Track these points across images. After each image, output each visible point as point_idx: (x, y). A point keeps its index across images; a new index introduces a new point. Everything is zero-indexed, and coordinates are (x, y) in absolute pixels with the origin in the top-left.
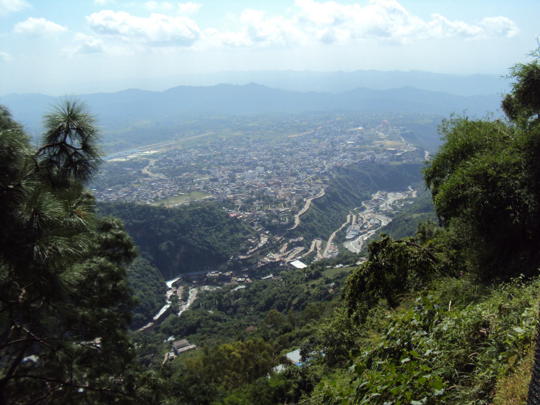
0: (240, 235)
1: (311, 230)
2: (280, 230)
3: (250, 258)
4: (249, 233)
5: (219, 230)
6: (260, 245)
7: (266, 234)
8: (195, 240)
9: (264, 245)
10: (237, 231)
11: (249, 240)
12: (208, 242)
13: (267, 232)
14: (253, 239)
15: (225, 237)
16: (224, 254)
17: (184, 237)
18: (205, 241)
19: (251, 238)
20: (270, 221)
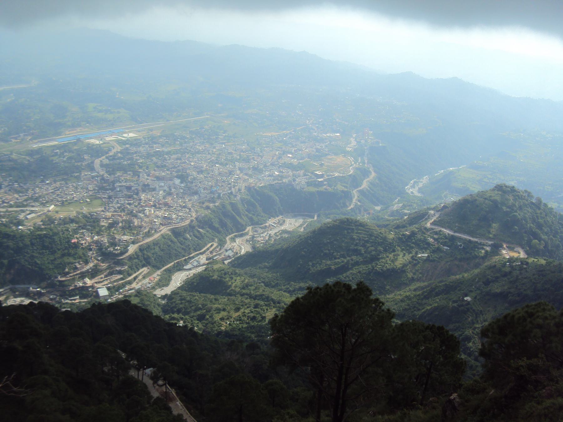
0: (71, 260)
1: (147, 258)
2: (111, 257)
3: (68, 280)
4: (80, 258)
5: (53, 253)
6: (85, 269)
7: (98, 260)
8: (26, 260)
9: (88, 270)
10: (69, 255)
11: (77, 264)
12: (37, 264)
13: (99, 258)
14: (80, 264)
15: (55, 259)
16: (47, 274)
17: (18, 257)
18: (36, 262)
19: (79, 262)
20: (106, 249)
